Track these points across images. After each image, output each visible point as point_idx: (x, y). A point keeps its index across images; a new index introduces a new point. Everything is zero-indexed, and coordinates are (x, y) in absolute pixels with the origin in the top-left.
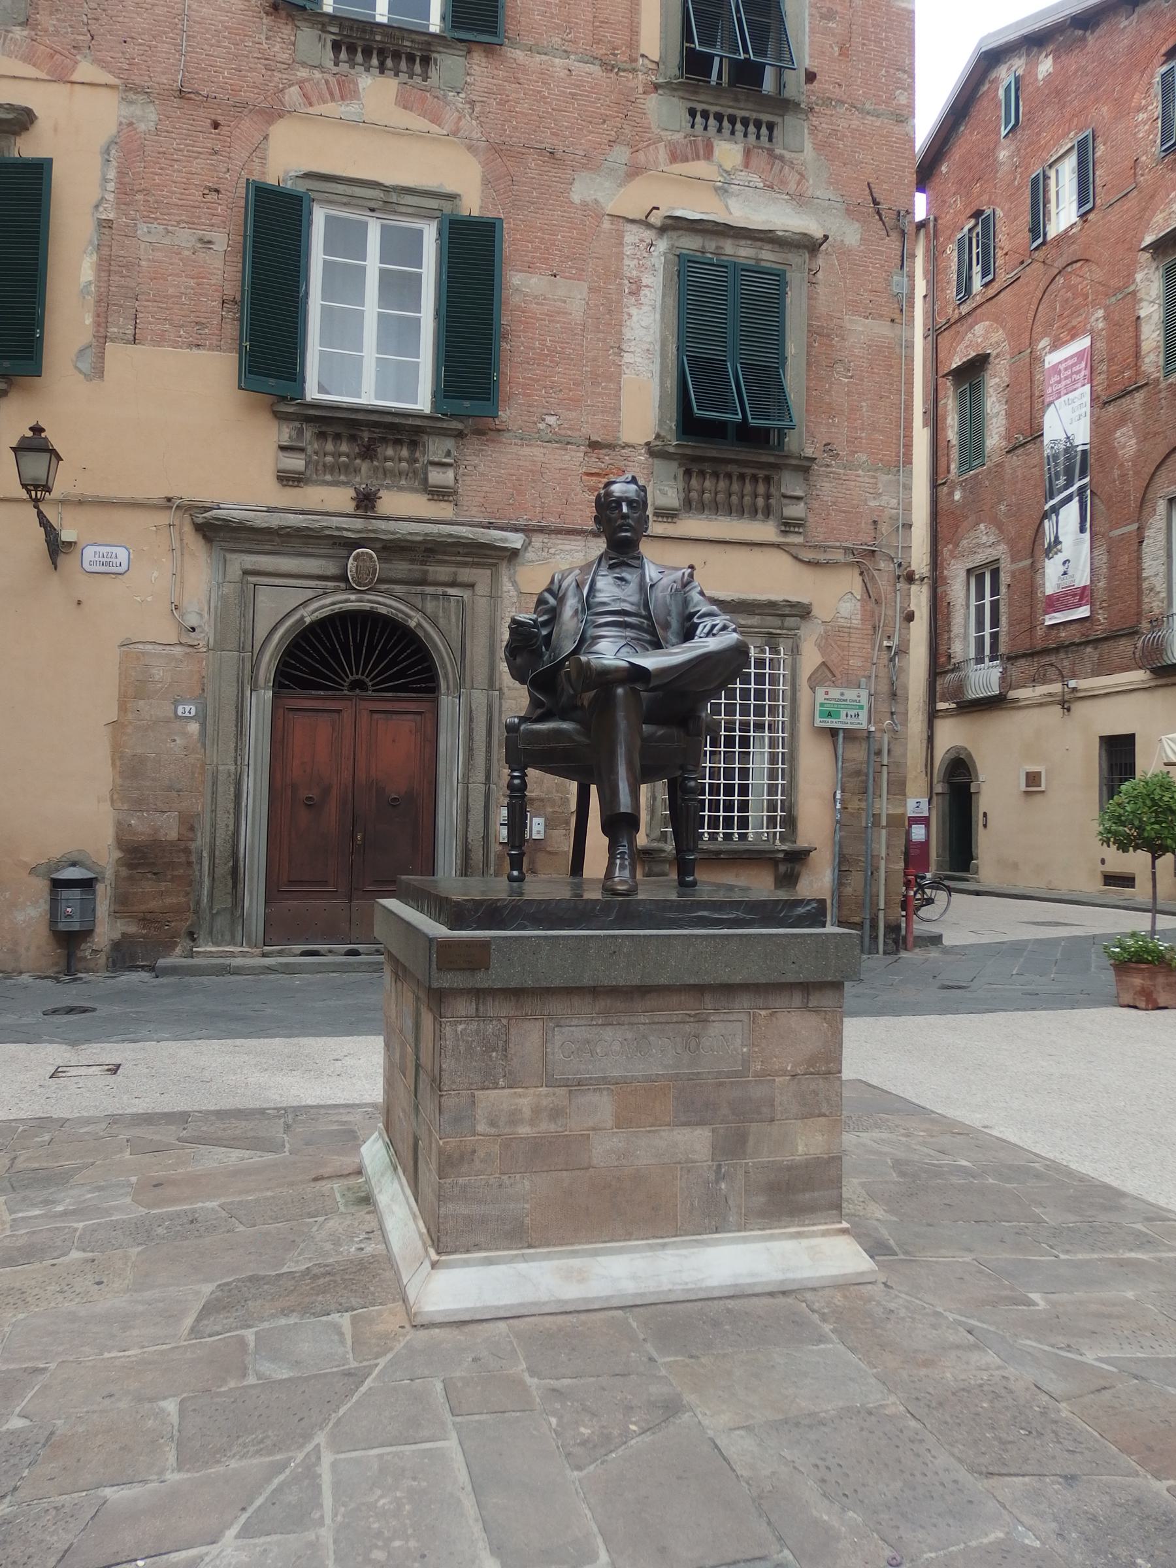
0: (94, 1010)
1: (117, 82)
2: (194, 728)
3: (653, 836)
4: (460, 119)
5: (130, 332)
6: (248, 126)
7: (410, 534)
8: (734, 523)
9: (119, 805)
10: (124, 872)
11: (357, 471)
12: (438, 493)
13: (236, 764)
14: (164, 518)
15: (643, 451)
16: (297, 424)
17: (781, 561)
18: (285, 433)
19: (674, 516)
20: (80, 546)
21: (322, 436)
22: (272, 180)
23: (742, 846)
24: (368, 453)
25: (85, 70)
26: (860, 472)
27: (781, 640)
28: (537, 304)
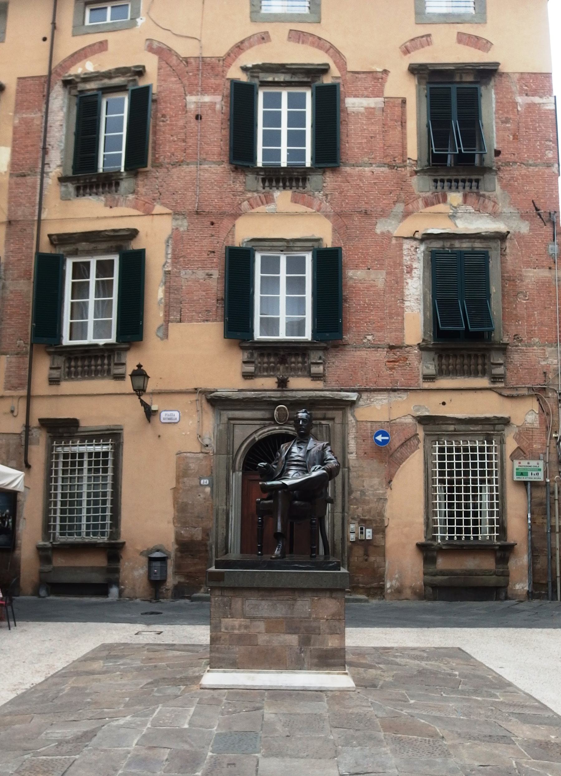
0: (161, 613)
1: (170, 211)
2: (208, 489)
3: (429, 537)
4: (321, 203)
5: (178, 317)
6: (226, 222)
7: (303, 397)
8: (466, 379)
9: (176, 525)
10: (179, 554)
11: (278, 369)
12: (316, 377)
13: (226, 505)
14: (194, 397)
15: (416, 348)
16: (251, 351)
17: (493, 397)
18: (245, 356)
19: (433, 379)
20: (159, 412)
21: (262, 355)
22: (237, 245)
23: (476, 543)
24: (283, 361)
25: (158, 208)
26: (535, 348)
27: (494, 437)
28: (361, 283)
